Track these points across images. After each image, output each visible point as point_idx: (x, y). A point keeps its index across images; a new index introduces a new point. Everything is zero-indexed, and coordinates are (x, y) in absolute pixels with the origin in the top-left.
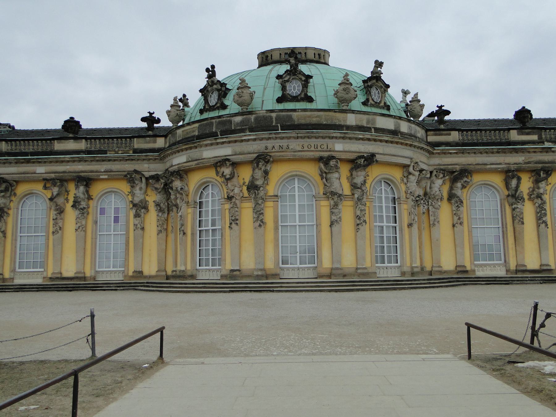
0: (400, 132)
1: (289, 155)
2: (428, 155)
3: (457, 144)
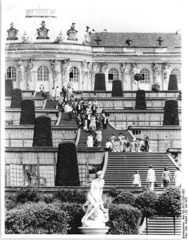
0: (80, 50)
2: (92, 57)
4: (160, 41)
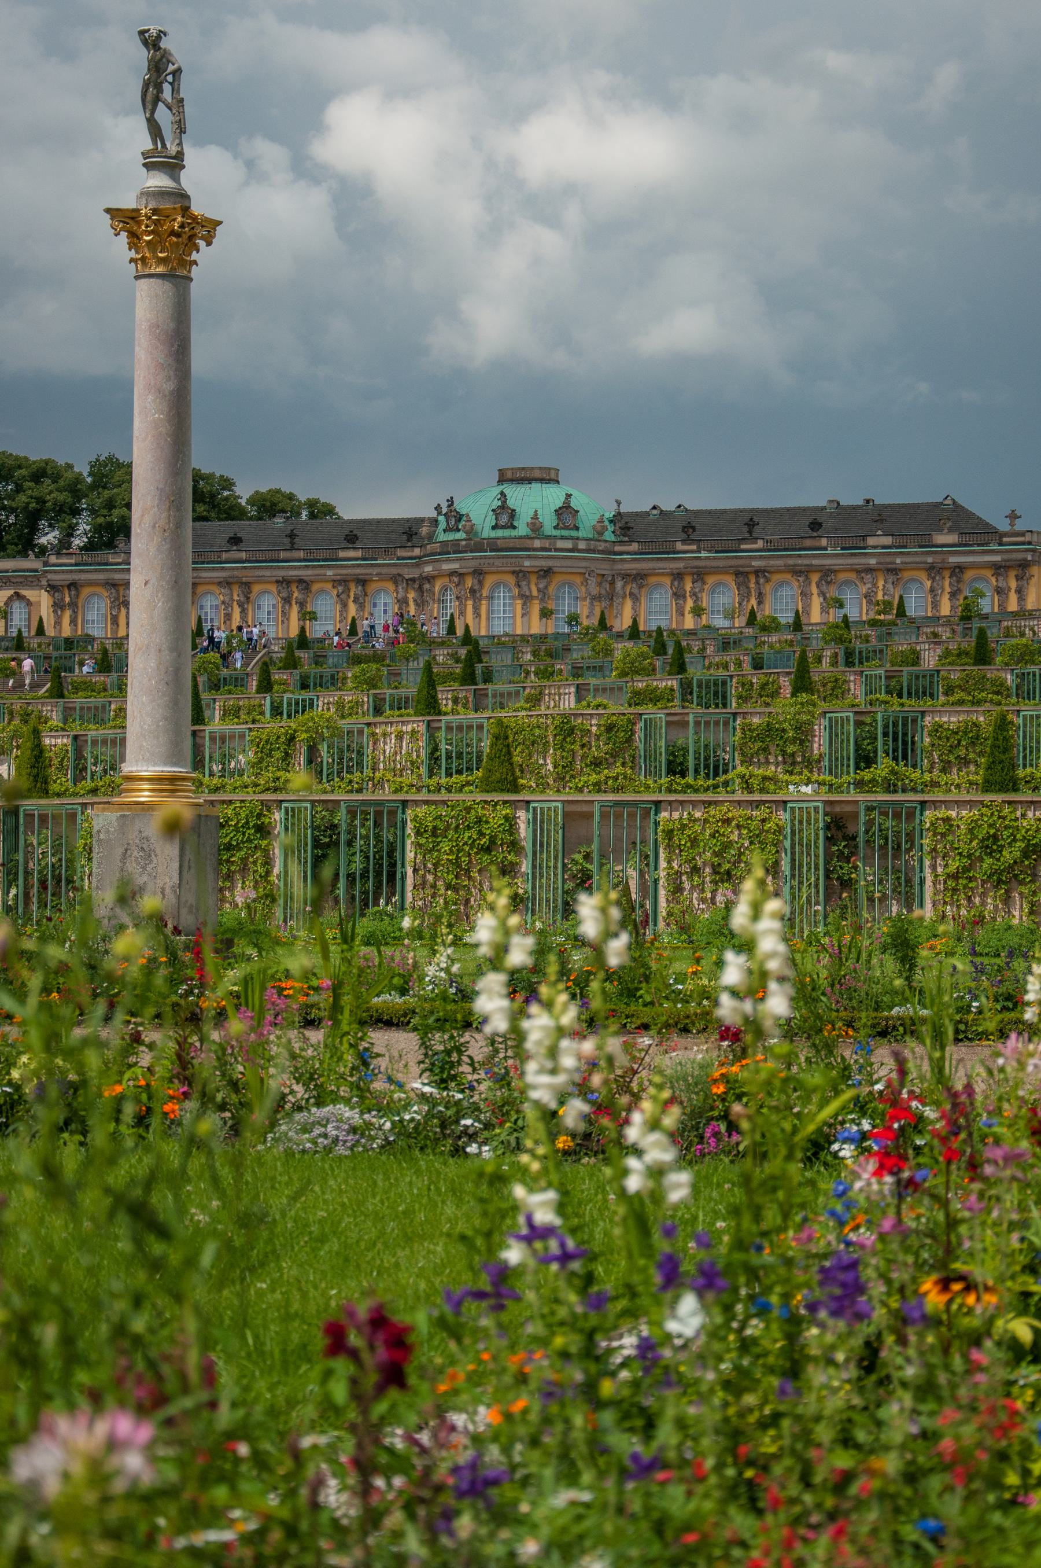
1: (494, 569)
3: (636, 554)
4: (751, 524)
